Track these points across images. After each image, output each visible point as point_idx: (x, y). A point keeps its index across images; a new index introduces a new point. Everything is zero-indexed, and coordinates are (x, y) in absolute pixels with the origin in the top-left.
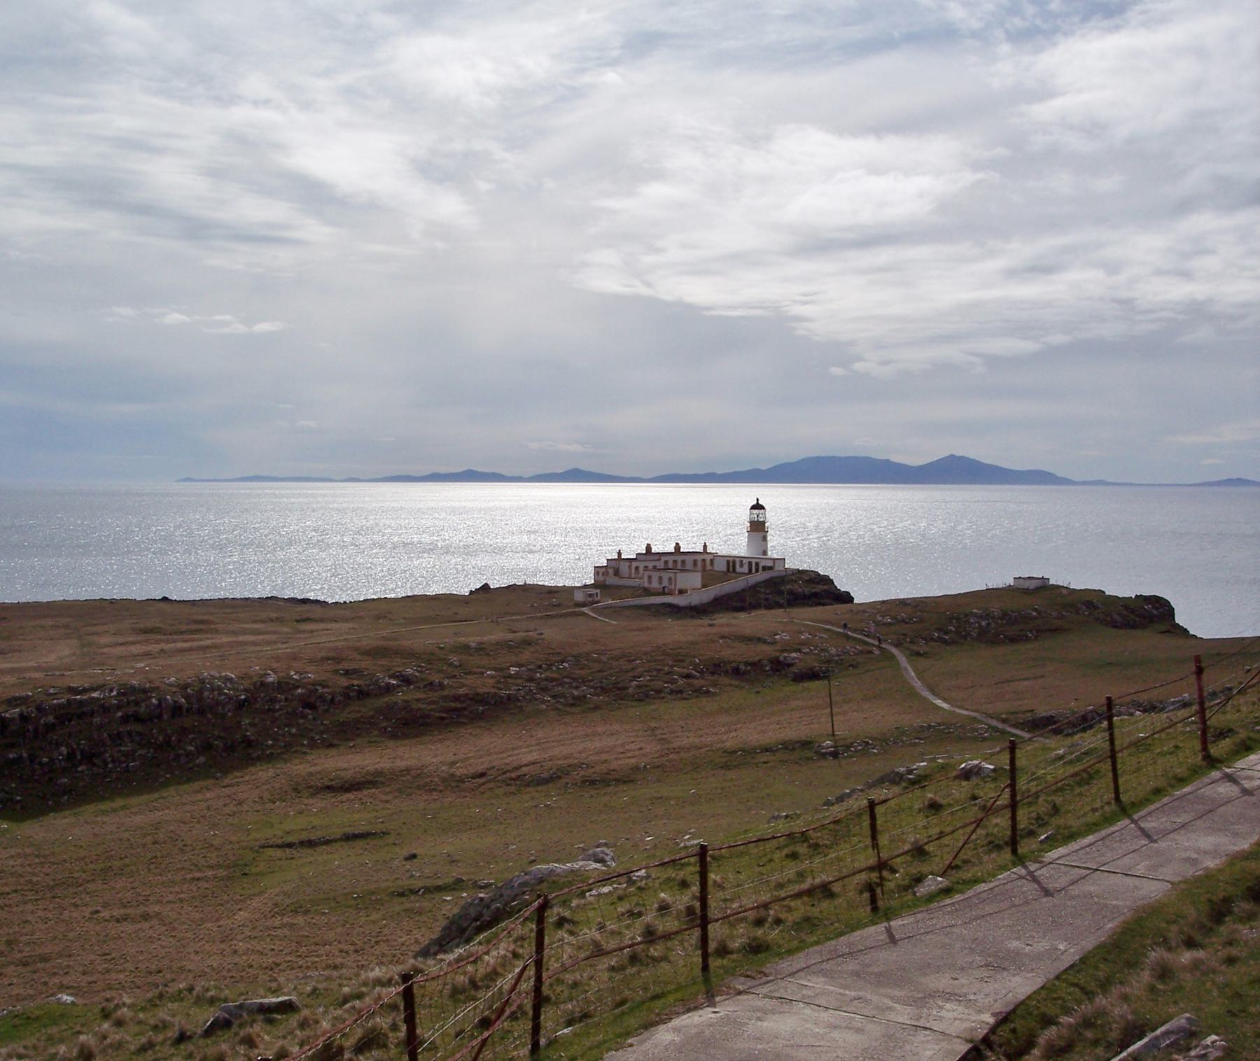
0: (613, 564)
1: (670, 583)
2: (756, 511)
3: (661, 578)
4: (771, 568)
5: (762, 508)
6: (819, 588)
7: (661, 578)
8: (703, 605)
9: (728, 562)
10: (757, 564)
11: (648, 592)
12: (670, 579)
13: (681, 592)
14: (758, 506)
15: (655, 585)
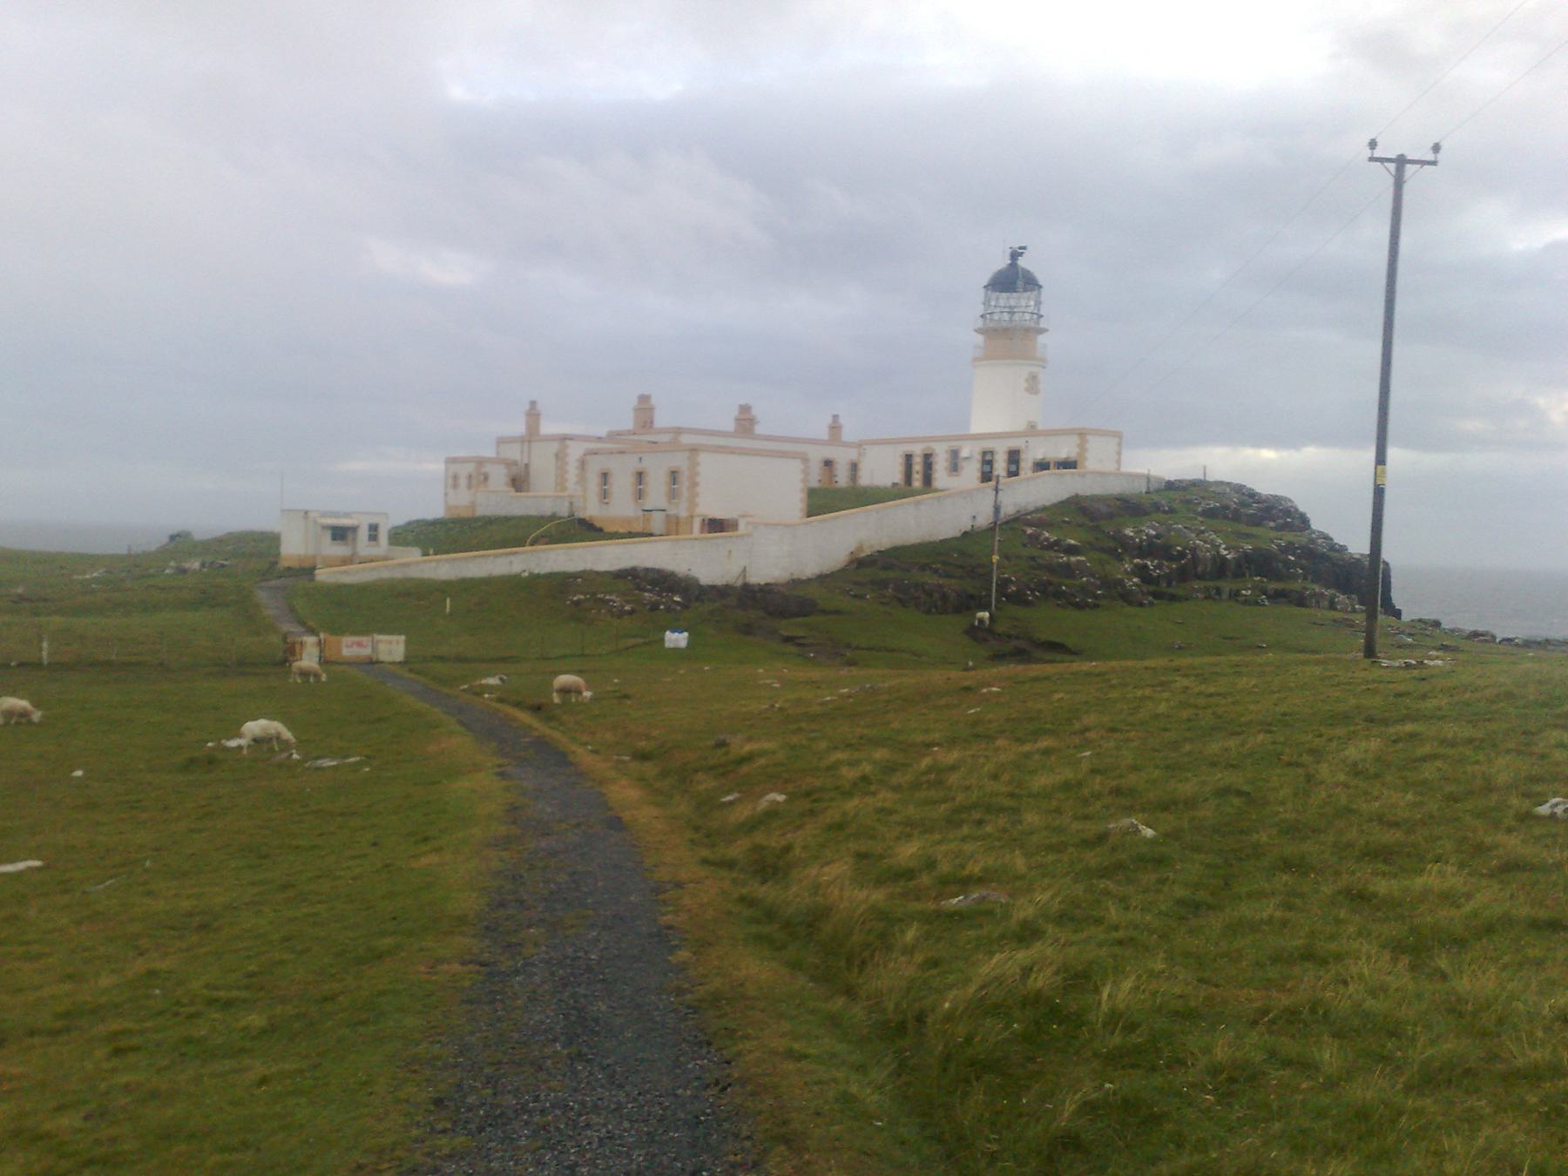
0: (513, 452)
1: (673, 495)
2: (1004, 299)
3: (640, 476)
4: (1068, 464)
5: (1031, 283)
6: (1270, 538)
7: (640, 476)
8: (796, 583)
9: (909, 458)
10: (1014, 457)
11: (587, 530)
12: (674, 476)
13: (716, 526)
14: (1012, 279)
15: (622, 507)
